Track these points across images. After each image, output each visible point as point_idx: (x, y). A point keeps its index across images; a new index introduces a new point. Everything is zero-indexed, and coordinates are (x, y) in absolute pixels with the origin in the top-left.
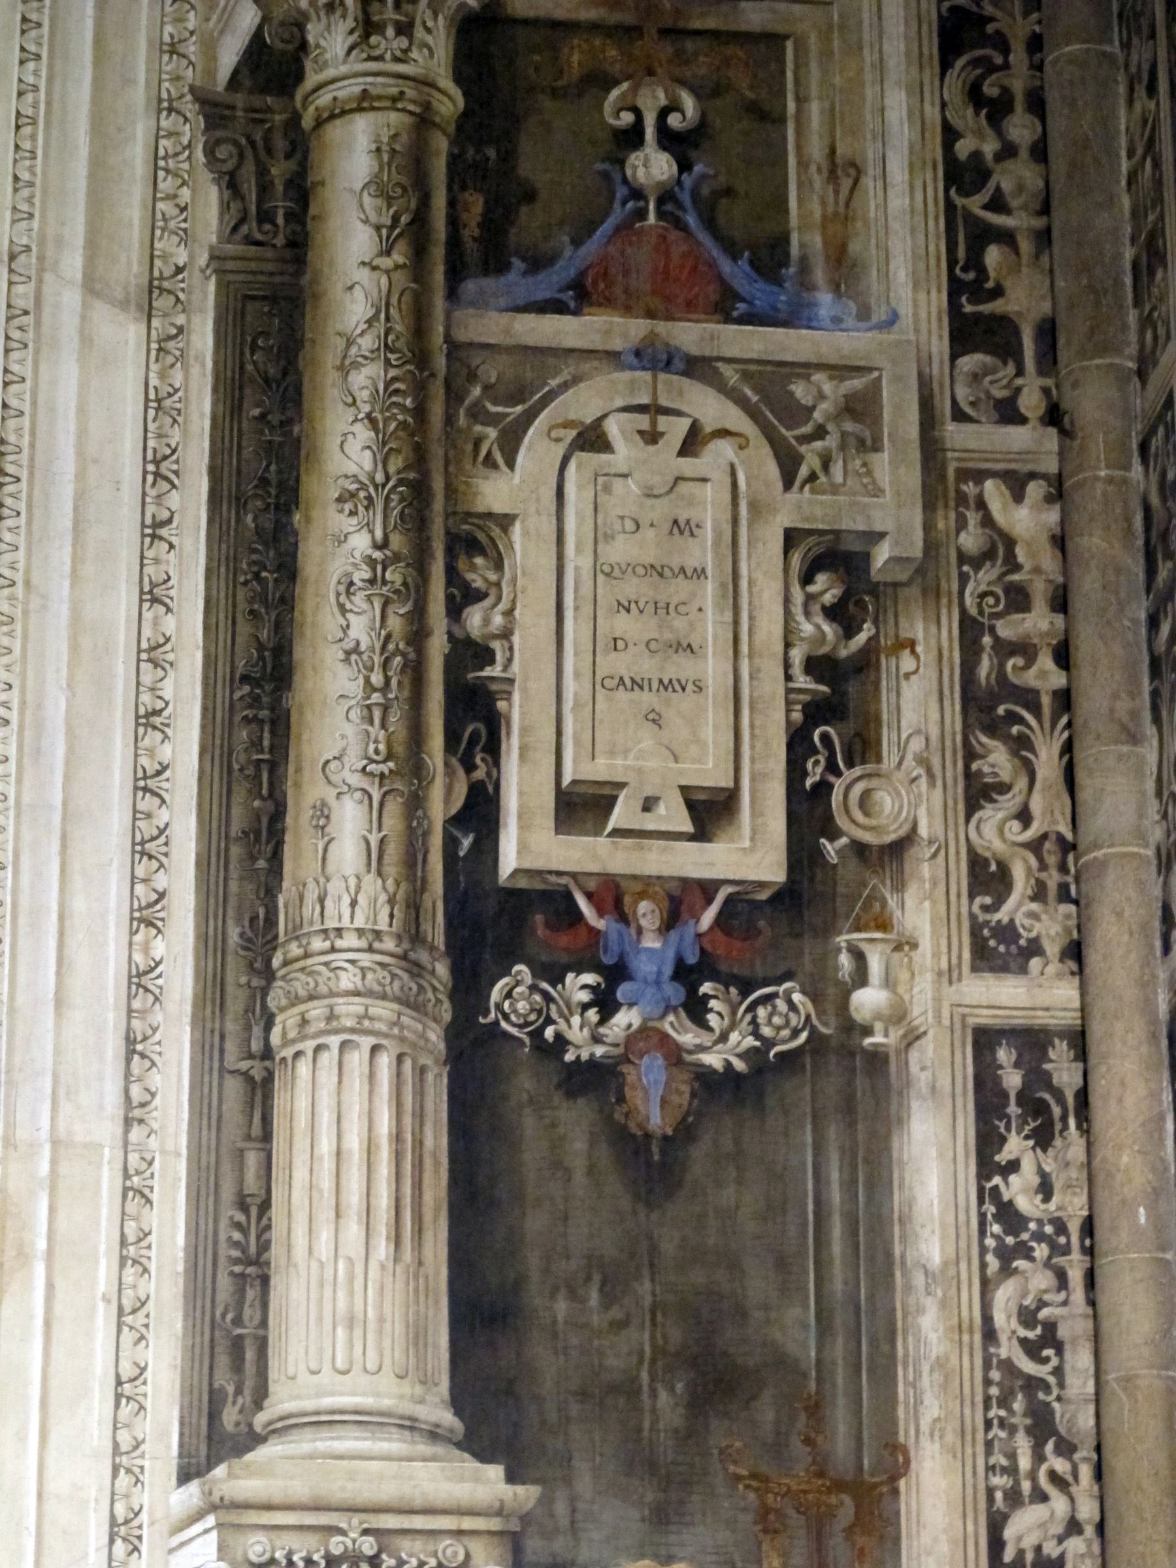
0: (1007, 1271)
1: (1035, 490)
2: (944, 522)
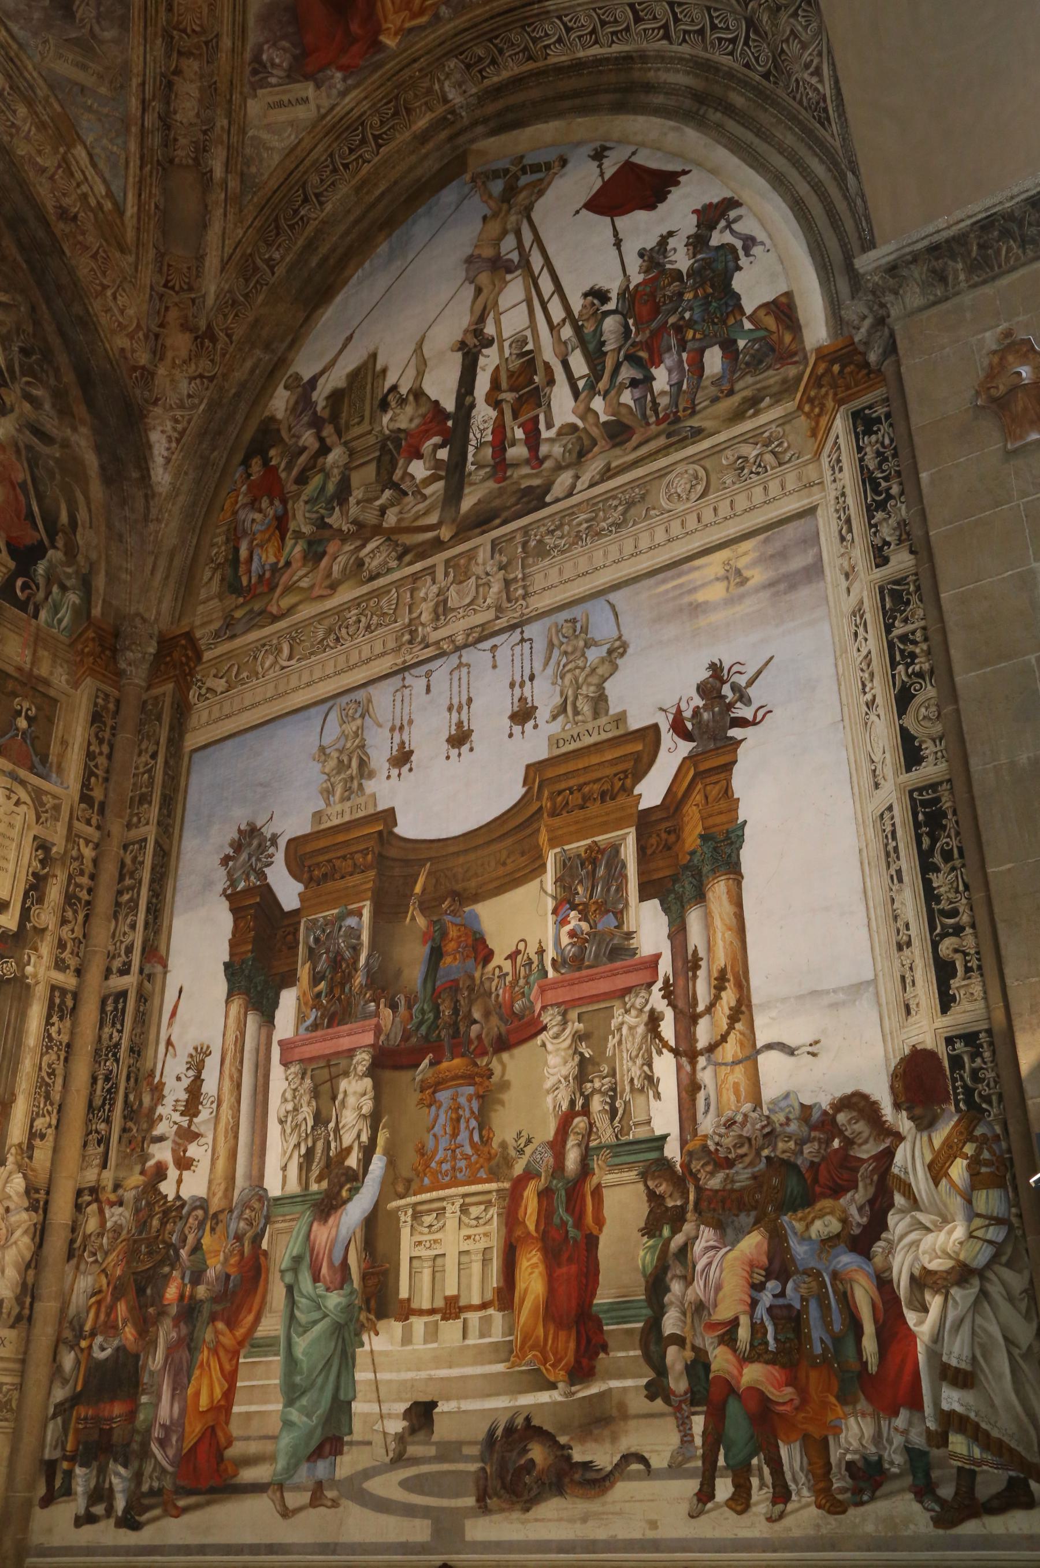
0: (47, 1053)
1: (91, 845)
2: (70, 846)
